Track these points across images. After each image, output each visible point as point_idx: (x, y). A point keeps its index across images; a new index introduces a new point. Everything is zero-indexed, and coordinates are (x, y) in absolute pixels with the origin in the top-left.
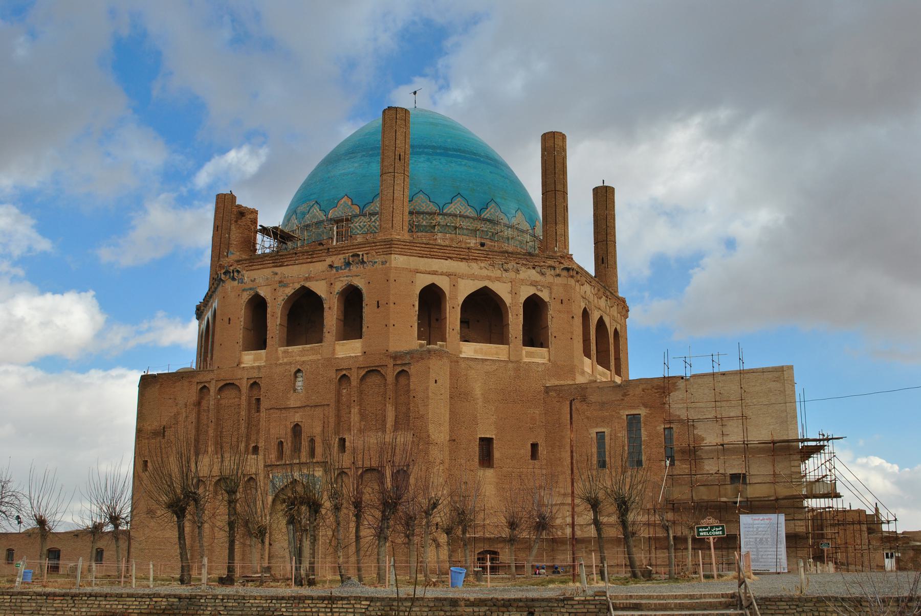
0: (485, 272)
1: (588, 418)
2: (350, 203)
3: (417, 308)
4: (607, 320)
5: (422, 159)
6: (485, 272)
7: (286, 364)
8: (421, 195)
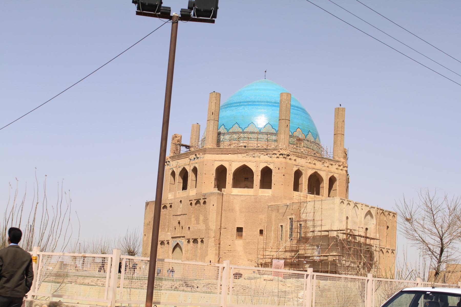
0: (245, 159)
3: (214, 175)
5: (241, 108)
6: (245, 159)
8: (236, 125)
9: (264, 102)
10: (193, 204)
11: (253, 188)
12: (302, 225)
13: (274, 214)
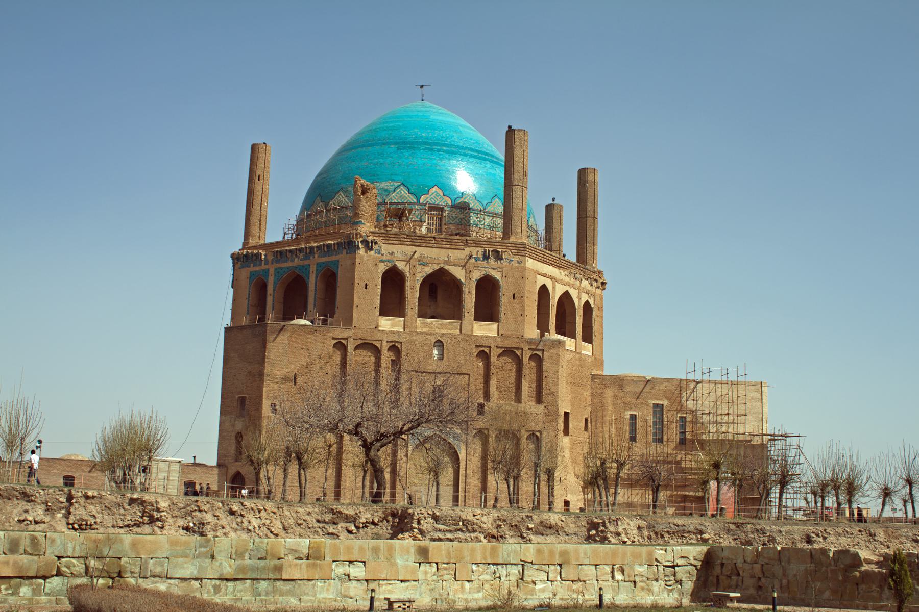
1: (624, 403)
7: (426, 333)
10: (493, 358)
12: (688, 419)
13: (609, 393)
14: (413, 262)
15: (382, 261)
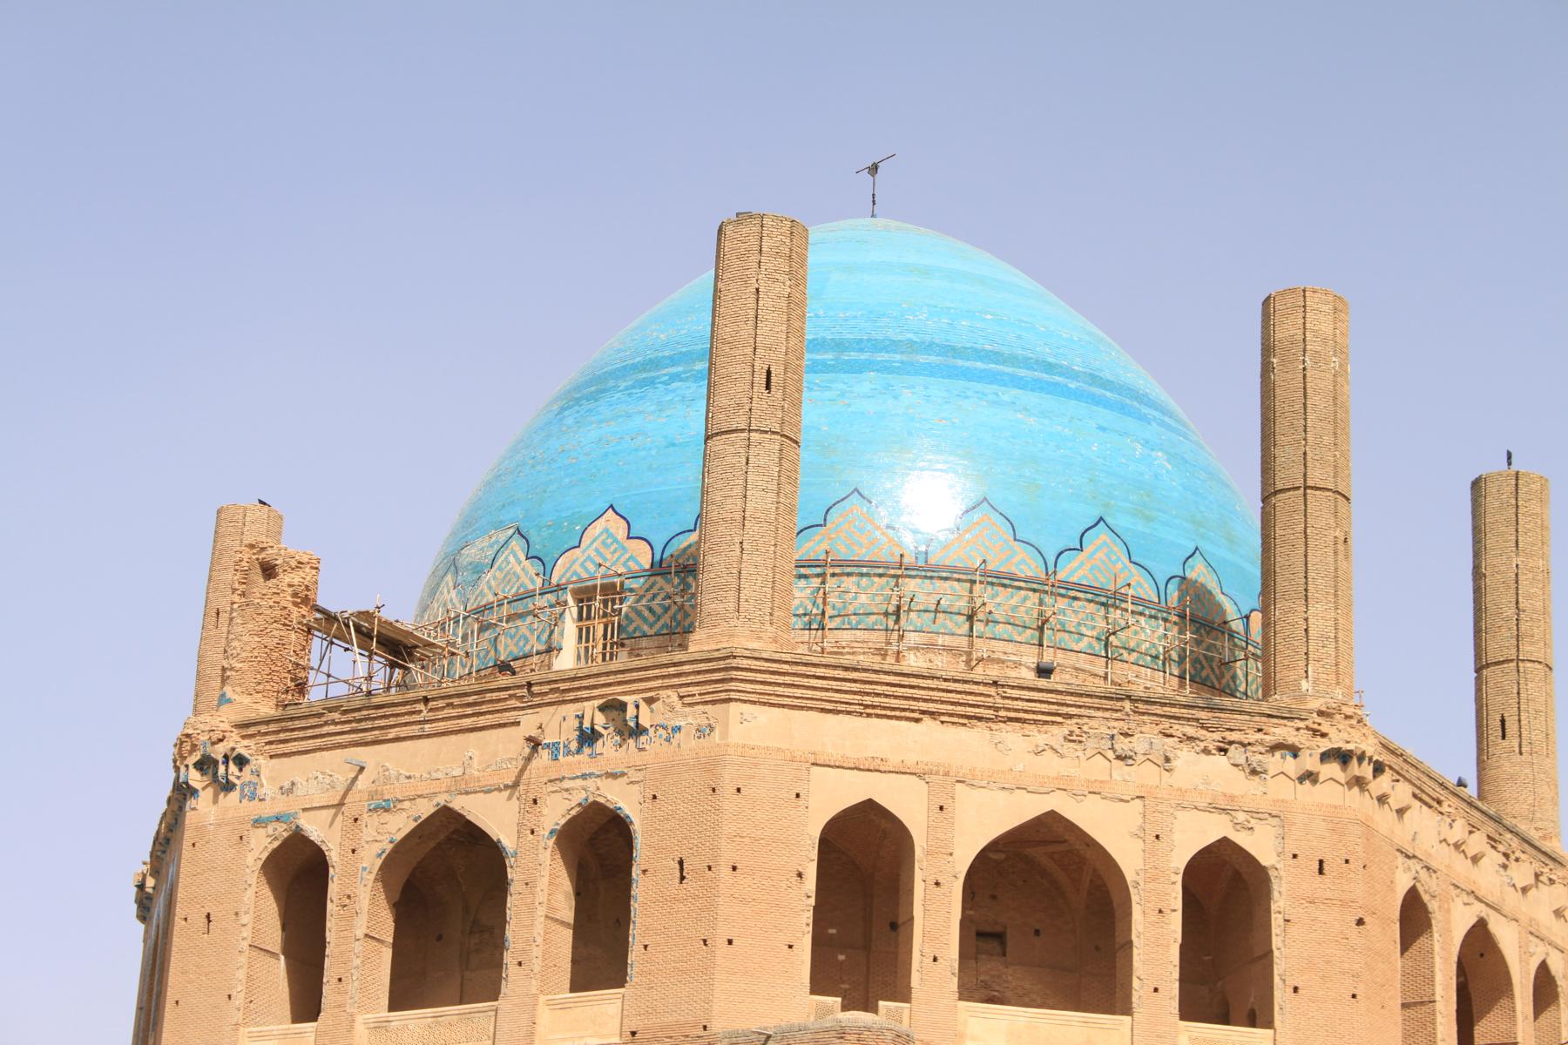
0: (1051, 766)
2: (621, 533)
4: (1506, 936)
6: (1051, 766)
9: (1026, 363)
11: (1127, 1010)
14: (349, 810)
15: (259, 823)
